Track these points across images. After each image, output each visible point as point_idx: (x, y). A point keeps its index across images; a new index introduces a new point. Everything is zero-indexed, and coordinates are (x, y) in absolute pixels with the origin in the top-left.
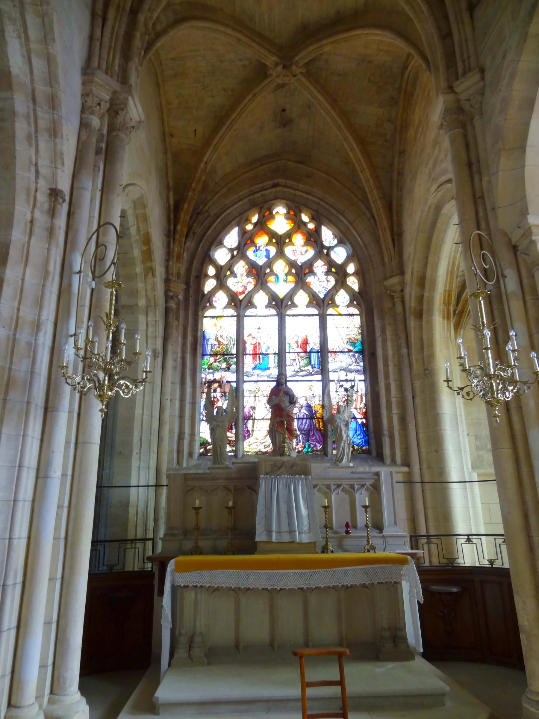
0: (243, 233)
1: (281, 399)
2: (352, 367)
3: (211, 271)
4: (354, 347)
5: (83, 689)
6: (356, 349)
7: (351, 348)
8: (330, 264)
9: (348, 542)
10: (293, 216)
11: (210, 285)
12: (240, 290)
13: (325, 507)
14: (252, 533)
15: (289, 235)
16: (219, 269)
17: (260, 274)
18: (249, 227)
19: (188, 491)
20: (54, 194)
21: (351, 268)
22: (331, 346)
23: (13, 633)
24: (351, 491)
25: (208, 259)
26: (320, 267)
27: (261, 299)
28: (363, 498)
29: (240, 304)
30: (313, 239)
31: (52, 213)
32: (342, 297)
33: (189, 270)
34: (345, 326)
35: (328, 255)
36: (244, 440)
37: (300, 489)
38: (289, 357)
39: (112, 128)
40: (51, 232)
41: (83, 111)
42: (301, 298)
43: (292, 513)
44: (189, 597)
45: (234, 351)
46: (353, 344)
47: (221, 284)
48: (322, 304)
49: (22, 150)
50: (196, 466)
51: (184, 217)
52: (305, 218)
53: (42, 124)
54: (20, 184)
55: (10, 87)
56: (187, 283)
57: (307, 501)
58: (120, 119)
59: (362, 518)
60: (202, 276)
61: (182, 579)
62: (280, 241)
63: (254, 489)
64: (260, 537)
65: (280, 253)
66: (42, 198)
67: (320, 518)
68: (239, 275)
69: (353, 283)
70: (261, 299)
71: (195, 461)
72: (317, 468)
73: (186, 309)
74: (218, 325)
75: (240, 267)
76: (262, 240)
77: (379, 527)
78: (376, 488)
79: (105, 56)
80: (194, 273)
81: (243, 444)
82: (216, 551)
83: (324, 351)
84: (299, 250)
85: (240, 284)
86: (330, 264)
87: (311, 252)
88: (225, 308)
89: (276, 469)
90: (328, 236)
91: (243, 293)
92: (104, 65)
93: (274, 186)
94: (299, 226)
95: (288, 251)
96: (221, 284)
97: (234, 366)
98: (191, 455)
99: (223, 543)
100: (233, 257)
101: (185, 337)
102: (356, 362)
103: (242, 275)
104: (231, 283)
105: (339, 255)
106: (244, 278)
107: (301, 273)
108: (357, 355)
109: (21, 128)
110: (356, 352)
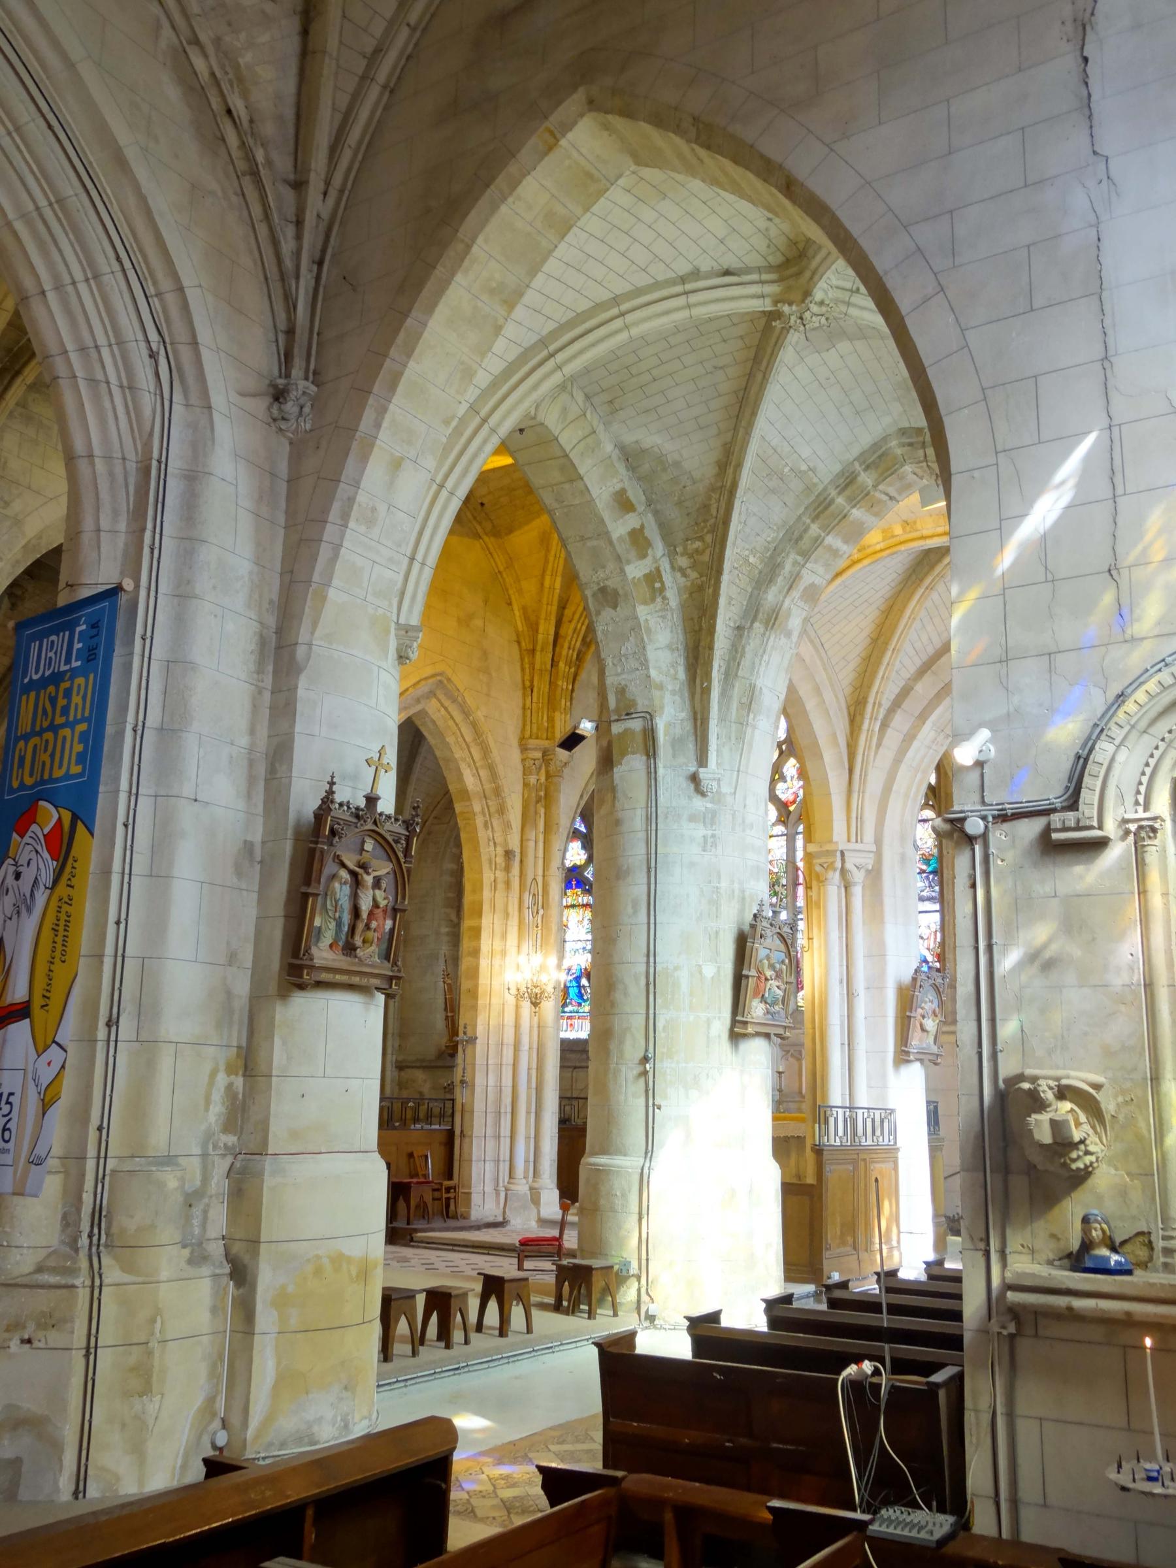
2: (924, 894)
4: (928, 864)
6: (930, 869)
7: (924, 867)
12: (791, 798)
13: (780, 1073)
20: (508, 854)
23: (508, 1140)
31: (507, 869)
36: (798, 992)
39: (548, 776)
40: (508, 884)
41: (524, 774)
46: (926, 861)
49: (482, 834)
53: (492, 809)
54: (484, 858)
55: (469, 799)
58: (552, 768)
66: (500, 860)
68: (788, 779)
79: (534, 720)
81: (796, 997)
85: (791, 791)
88: (774, 825)
91: (794, 802)
92: (535, 730)
102: (930, 886)
103: (792, 778)
106: (795, 782)
108: (931, 877)
109: (479, 821)
110: (930, 873)
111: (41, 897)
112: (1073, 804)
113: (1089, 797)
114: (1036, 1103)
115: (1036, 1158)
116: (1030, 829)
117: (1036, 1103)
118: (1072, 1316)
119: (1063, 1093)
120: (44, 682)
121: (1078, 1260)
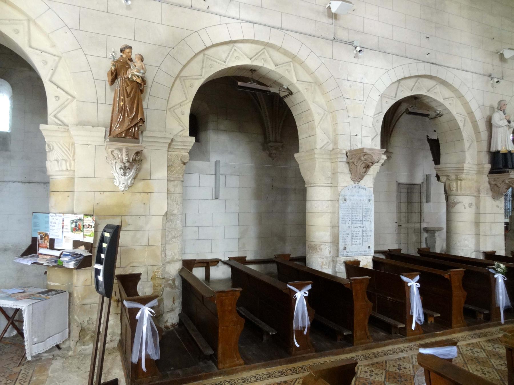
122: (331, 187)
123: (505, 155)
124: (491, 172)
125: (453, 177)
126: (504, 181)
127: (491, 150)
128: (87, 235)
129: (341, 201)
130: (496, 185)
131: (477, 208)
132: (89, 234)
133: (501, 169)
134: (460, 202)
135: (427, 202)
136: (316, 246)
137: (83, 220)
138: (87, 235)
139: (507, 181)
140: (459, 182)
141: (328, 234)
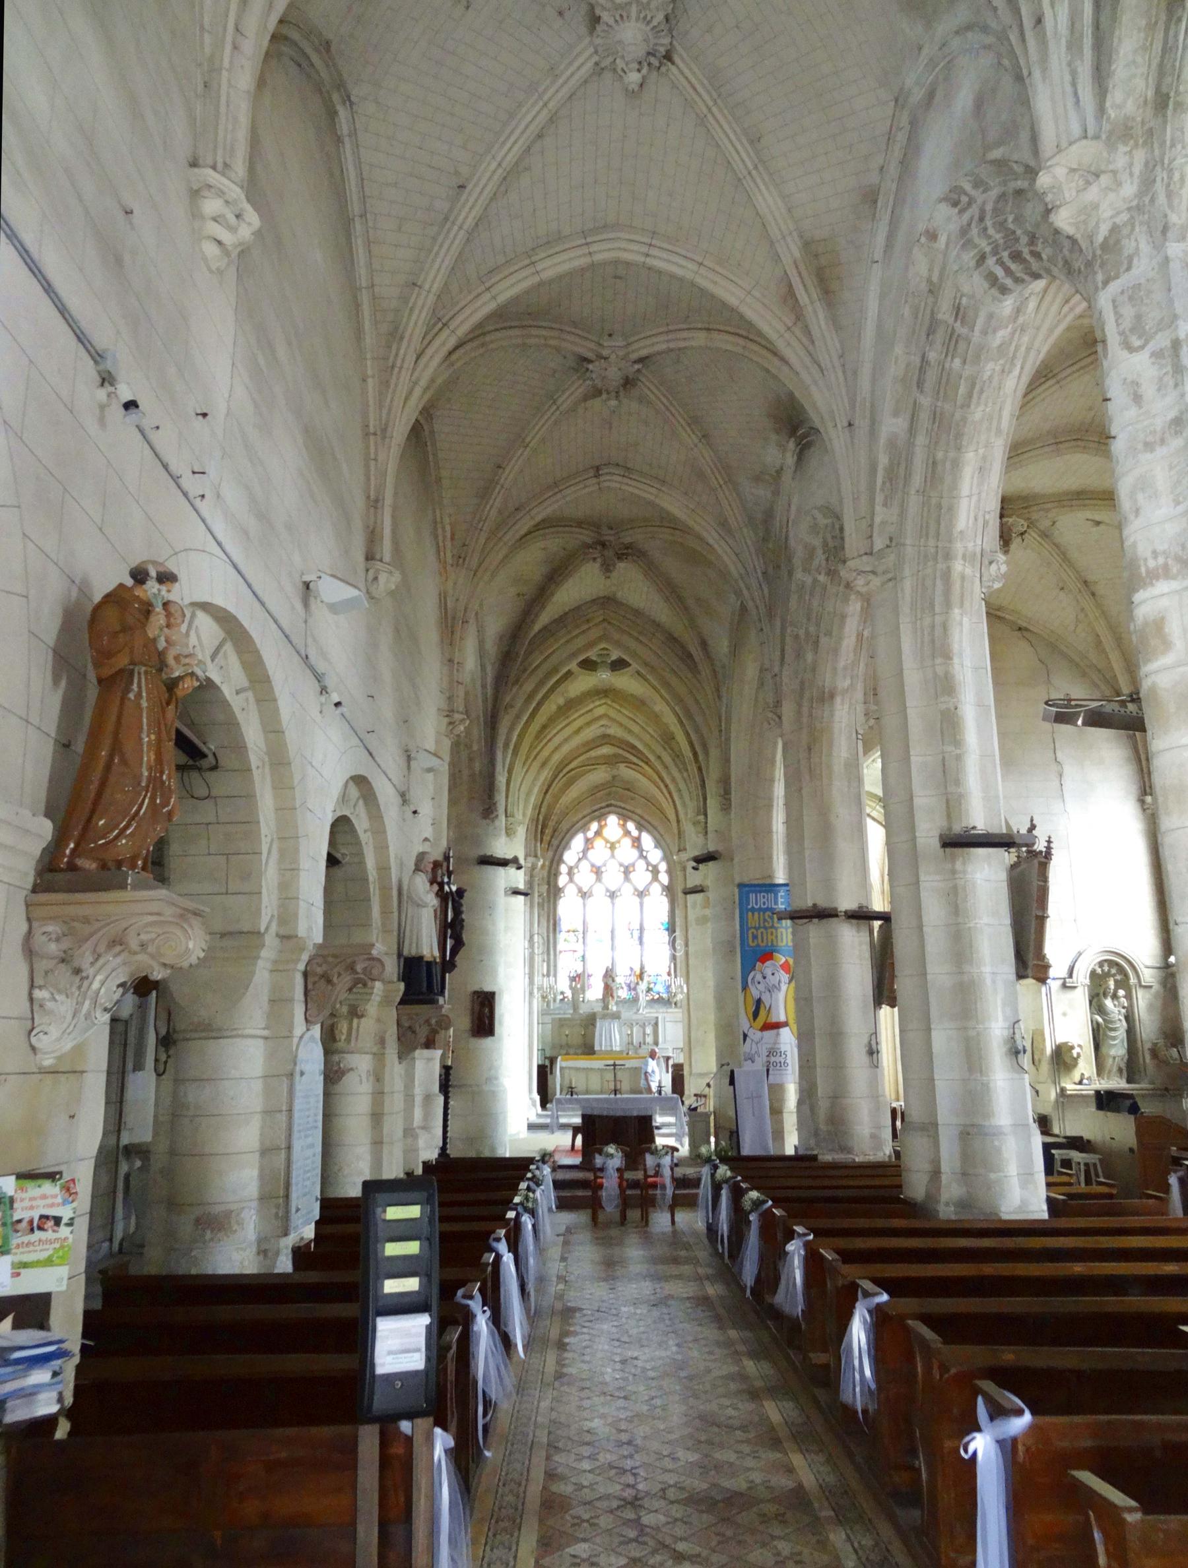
0: (588, 841)
1: (609, 975)
3: (563, 869)
5: (539, 1092)
8: (648, 864)
9: (640, 1051)
10: (624, 826)
11: (562, 880)
14: (593, 1047)
15: (619, 842)
16: (571, 869)
17: (598, 872)
18: (590, 834)
19: (561, 1026)
21: (663, 867)
22: (645, 926)
24: (644, 1026)
25: (560, 860)
26: (641, 864)
27: (599, 890)
28: (649, 1030)
29: (584, 895)
30: (637, 843)
32: (656, 889)
33: (549, 872)
34: (658, 906)
35: (645, 858)
37: (615, 1026)
38: (616, 933)
42: (627, 889)
43: (611, 1037)
44: (567, 1072)
45: (581, 929)
47: (571, 880)
48: (641, 894)
50: (560, 1008)
51: (547, 838)
52: (631, 826)
56: (549, 883)
57: (620, 1032)
59: (649, 1040)
60: (557, 874)
61: (564, 1064)
62: (613, 847)
63: (594, 1025)
64: (597, 1048)
65: (613, 856)
67: (625, 1039)
69: (664, 878)
70: (599, 890)
71: (558, 1004)
72: (625, 1015)
73: (549, 901)
74: (568, 907)
75: (585, 866)
76: (599, 843)
77: (656, 1043)
78: (656, 1024)
80: (553, 872)
82: (576, 1054)
83: (642, 929)
84: (627, 852)
86: (648, 864)
87: (635, 853)
89: (604, 1017)
90: (647, 840)
93: (608, 806)
94: (627, 833)
95: (616, 852)
96: (571, 880)
97: (581, 940)
98: (555, 1000)
99: (579, 1051)
100: (580, 859)
101: (548, 921)
104: (576, 878)
105: (655, 855)
107: (627, 871)
111: (784, 987)
112: (1071, 976)
113: (1074, 975)
114: (1072, 1048)
115: (1068, 1060)
116: (1060, 982)
117: (1072, 1048)
118: (1082, 1096)
119: (1080, 1046)
120: (760, 909)
121: (1080, 1083)
122: (266, 1038)
123: (429, 964)
124: (403, 1002)
125: (345, 1009)
126: (427, 1022)
127: (406, 953)
128: (25, 1265)
129: (297, 1077)
130: (410, 1027)
131: (378, 1080)
132: (43, 1256)
133: (422, 994)
134: (352, 1069)
135: (134, 1070)
136: (228, 1214)
137: (12, 1200)
138: (25, 1265)
139: (433, 1021)
140: (355, 1021)
141: (255, 1173)
